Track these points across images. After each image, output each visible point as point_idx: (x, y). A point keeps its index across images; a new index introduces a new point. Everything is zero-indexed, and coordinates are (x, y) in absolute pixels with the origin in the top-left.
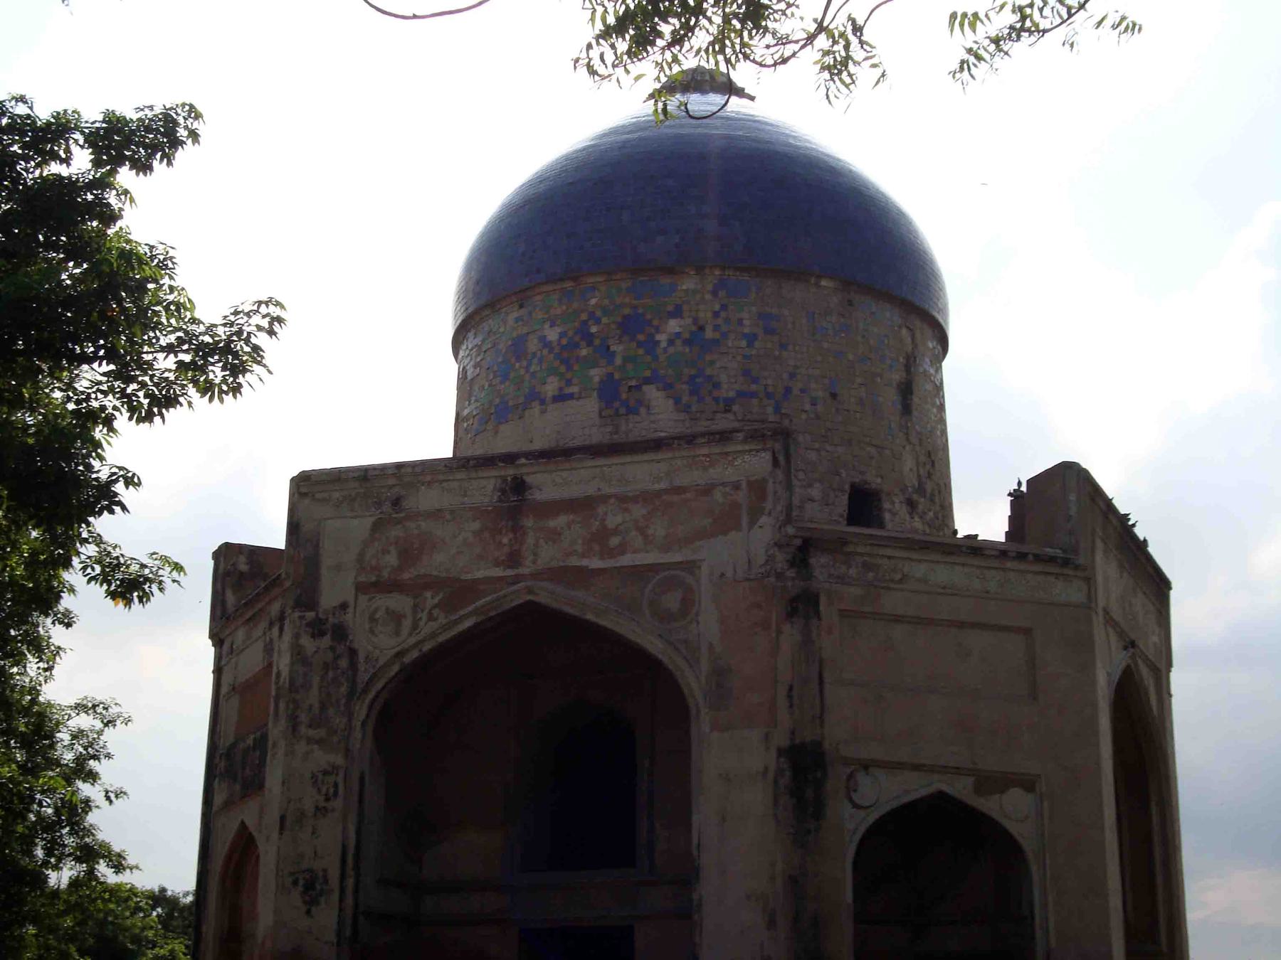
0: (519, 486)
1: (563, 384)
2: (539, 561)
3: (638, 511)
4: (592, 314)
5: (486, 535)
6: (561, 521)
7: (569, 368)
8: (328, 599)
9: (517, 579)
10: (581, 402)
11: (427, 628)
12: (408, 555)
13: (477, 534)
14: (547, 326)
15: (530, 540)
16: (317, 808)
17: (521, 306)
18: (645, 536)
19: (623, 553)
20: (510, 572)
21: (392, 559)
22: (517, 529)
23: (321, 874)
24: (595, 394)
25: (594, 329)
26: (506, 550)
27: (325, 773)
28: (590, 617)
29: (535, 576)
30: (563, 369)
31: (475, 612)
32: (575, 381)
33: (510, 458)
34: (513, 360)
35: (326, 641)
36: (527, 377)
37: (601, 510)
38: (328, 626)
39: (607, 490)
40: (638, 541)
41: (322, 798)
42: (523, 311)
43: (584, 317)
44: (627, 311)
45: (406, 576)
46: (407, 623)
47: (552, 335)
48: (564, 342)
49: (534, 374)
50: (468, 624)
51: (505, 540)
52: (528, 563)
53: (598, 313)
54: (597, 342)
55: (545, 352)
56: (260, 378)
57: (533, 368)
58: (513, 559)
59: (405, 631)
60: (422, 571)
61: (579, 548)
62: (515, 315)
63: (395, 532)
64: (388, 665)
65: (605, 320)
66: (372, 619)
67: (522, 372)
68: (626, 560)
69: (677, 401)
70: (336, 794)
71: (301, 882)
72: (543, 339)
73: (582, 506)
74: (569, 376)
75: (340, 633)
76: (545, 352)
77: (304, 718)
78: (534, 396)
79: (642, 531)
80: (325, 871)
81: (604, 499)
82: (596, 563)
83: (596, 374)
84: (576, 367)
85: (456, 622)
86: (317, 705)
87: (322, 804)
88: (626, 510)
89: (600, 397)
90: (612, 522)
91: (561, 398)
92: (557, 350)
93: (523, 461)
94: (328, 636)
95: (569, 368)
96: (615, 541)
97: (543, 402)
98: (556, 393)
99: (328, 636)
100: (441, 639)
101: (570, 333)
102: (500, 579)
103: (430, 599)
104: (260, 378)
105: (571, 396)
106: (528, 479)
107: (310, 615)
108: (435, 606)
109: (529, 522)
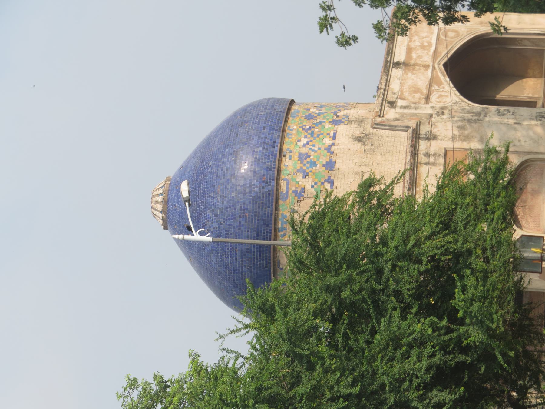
0: (397, 65)
1: (328, 136)
2: (429, 61)
3: (416, 38)
4: (300, 127)
5: (414, 72)
6: (414, 55)
7: (322, 134)
8: (430, 111)
9: (434, 68)
10: (338, 130)
11: (447, 88)
12: (416, 90)
13: (413, 74)
14: (299, 143)
15: (420, 62)
16: (513, 114)
17: (285, 156)
18: (426, 37)
19: (431, 43)
20: (431, 68)
21: (418, 95)
22: (414, 65)
23: (538, 114)
24: (336, 126)
25: (308, 127)
26: (422, 68)
27: (499, 112)
28: (452, 52)
29: (434, 63)
30: (321, 136)
31: (444, 76)
32: (328, 132)
33: (386, 62)
34: (308, 160)
35: (446, 112)
36: (319, 152)
37: (413, 46)
38: (440, 111)
39: (406, 44)
40: (428, 39)
41: (509, 113)
42: (287, 156)
43: (301, 129)
44: (303, 118)
45: (425, 91)
46: (443, 94)
47: (304, 141)
48: (309, 136)
49: (319, 149)
50: (448, 79)
51: (418, 68)
52: (427, 63)
53: (301, 125)
54: (314, 126)
55: (310, 143)
56: (344, 88)
57: (316, 149)
58: (426, 67)
59: (446, 94)
60: (424, 87)
61: (426, 52)
62: (287, 160)
63: (406, 94)
64: (459, 98)
65: (304, 124)
66: (440, 102)
67: (316, 154)
68: (434, 42)
69: (347, 109)
70: (508, 110)
71: (540, 119)
72: (304, 145)
73: (409, 50)
74: (325, 134)
75: (443, 108)
76: (310, 143)
77: (476, 118)
78: (329, 149)
79: (424, 38)
80: (537, 113)
81: (408, 45)
82: (433, 49)
83: (328, 126)
84: (322, 132)
85: (447, 82)
86: (472, 114)
87: (511, 113)
88: (414, 41)
89: (339, 124)
90: (418, 44)
91: (334, 137)
92: (312, 139)
93: (389, 59)
94: (444, 111)
95: (322, 134)
96: (426, 44)
97: (333, 144)
98: (331, 138)
99: (444, 111)
100: (452, 85)
101: (306, 134)
102: (432, 70)
103: (435, 87)
104: (344, 88)
105: (335, 134)
106: (395, 61)
107: (434, 116)
108: (439, 87)
109: (412, 62)
